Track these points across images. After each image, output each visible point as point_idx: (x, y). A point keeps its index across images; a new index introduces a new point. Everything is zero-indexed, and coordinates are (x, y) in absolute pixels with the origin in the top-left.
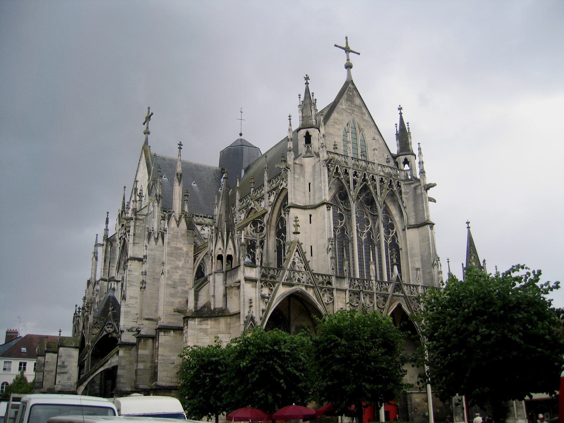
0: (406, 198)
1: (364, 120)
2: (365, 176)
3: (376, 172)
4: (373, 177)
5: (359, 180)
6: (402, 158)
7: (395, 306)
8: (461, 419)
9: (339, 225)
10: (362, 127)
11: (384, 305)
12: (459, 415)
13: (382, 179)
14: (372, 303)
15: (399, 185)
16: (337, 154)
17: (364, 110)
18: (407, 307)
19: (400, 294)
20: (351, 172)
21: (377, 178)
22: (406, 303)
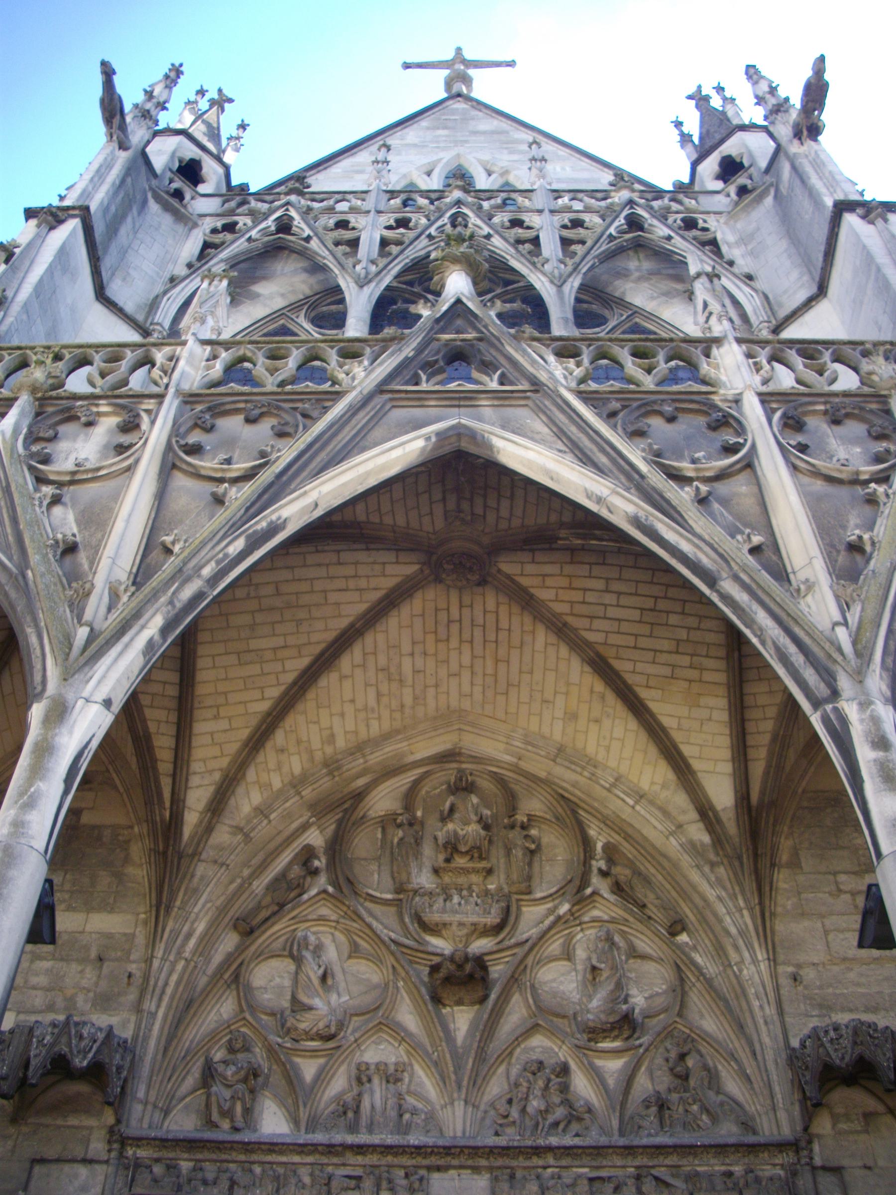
0: (743, 241)
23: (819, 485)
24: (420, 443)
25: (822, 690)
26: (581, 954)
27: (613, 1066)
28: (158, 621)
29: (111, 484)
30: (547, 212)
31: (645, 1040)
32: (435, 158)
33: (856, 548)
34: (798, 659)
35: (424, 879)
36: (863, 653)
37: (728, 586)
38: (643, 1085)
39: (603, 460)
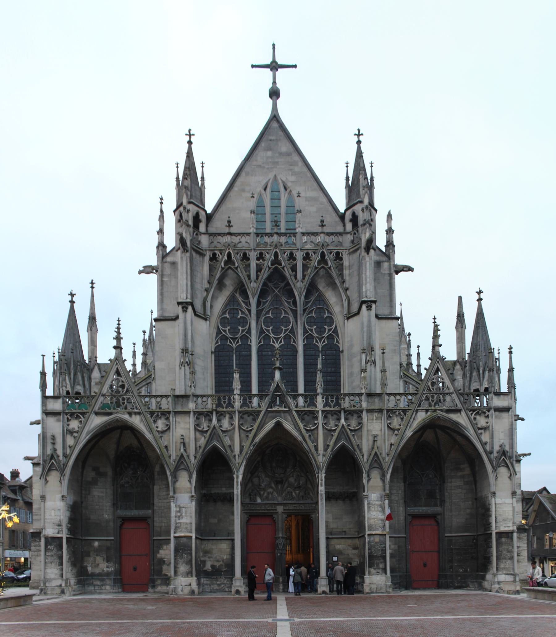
1: (294, 173)
2: (276, 255)
3: (299, 246)
4: (291, 254)
5: (267, 263)
6: (349, 215)
7: (270, 426)
8: (380, 571)
9: (223, 329)
10: (289, 184)
11: (252, 426)
12: (378, 565)
13: (307, 254)
14: (232, 424)
15: (338, 257)
16: (230, 234)
17: (296, 158)
18: (293, 425)
19: (280, 409)
20: (253, 256)
21: (299, 256)
22: (292, 420)
23: (326, 431)
24: (273, 425)
25: (317, 472)
26: (294, 476)
27: (297, 492)
28: (245, 462)
29: (232, 431)
30: (299, 250)
31: (301, 489)
32: (267, 180)
33: (328, 445)
34: (316, 467)
35: (274, 465)
36: (323, 467)
37: (310, 454)
38: (301, 494)
39: (297, 428)
